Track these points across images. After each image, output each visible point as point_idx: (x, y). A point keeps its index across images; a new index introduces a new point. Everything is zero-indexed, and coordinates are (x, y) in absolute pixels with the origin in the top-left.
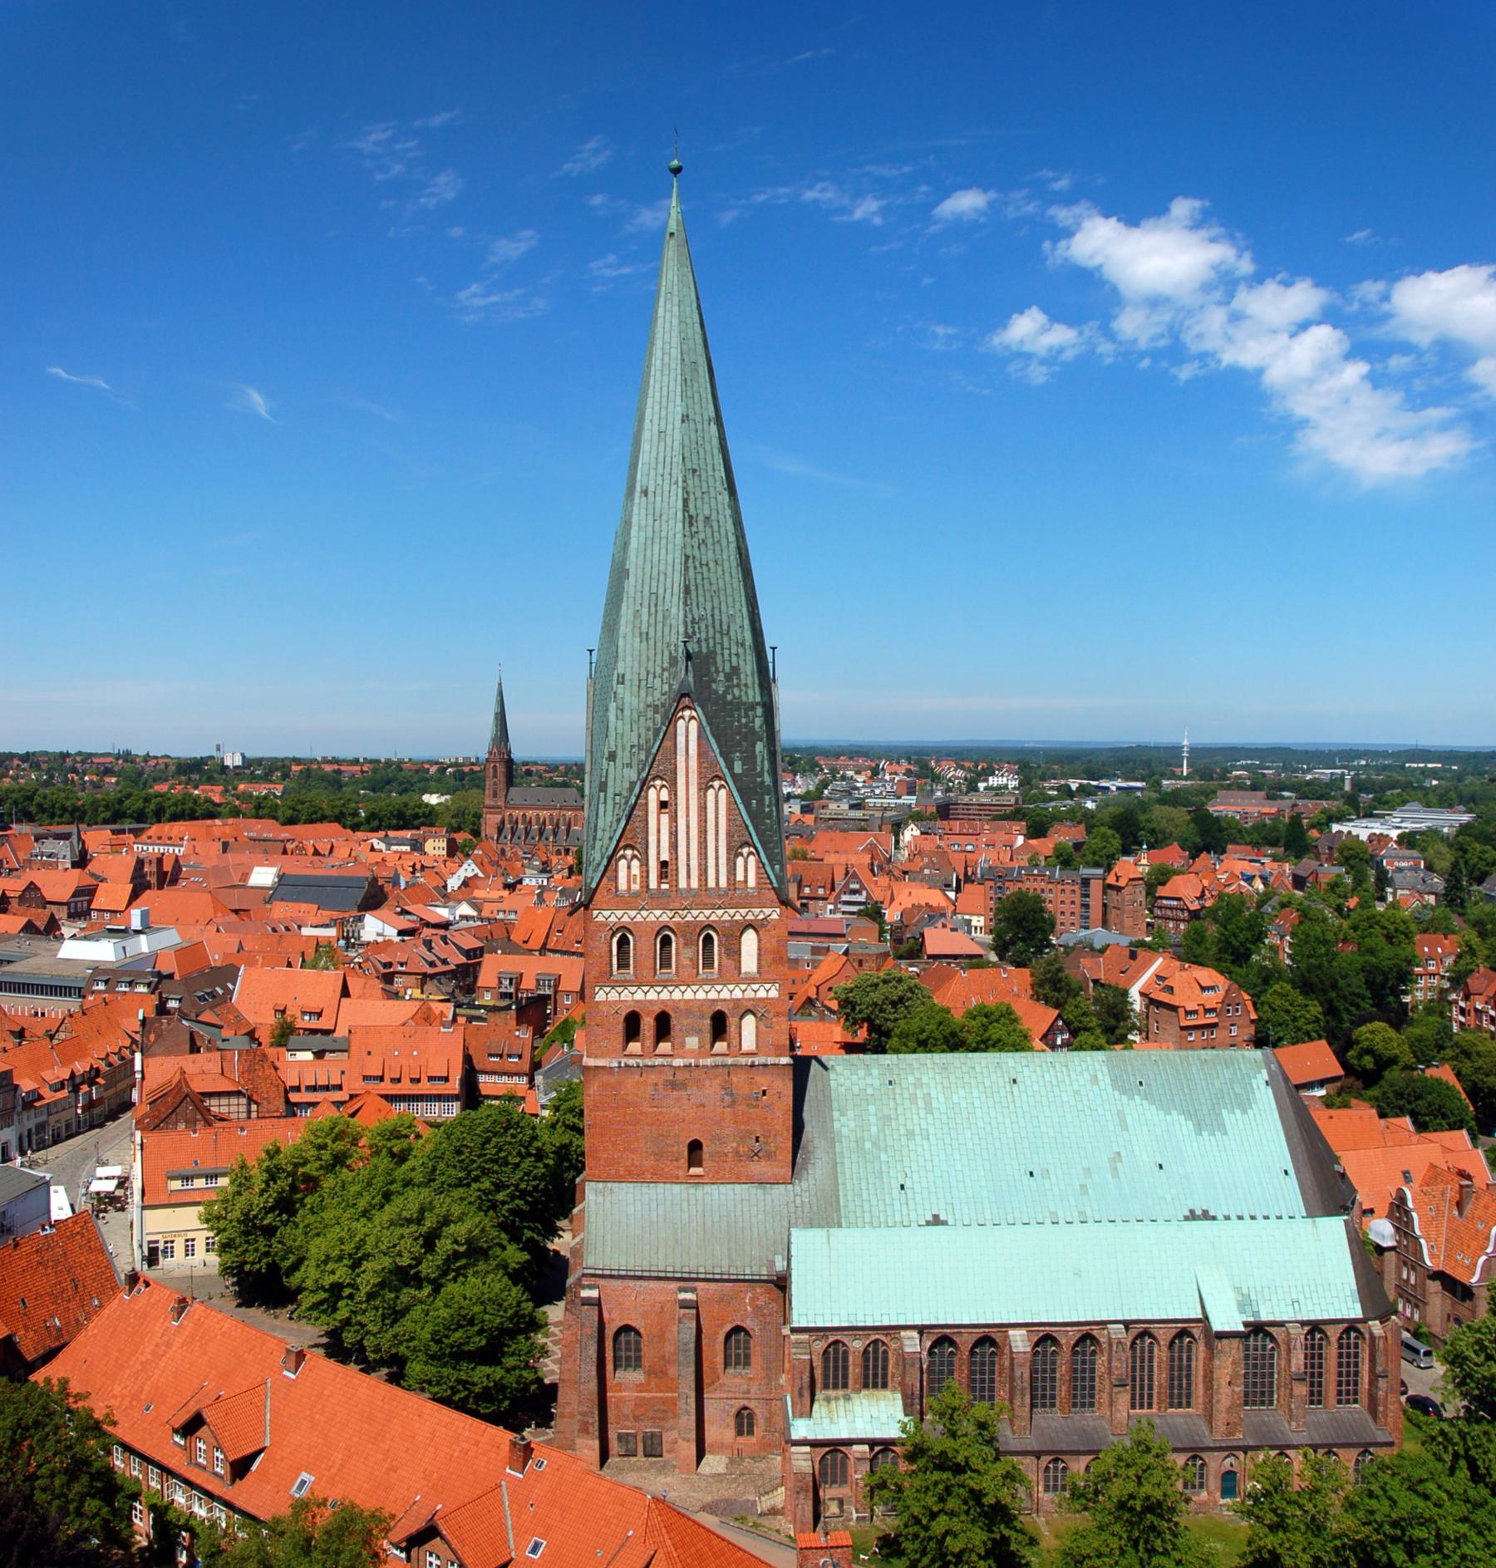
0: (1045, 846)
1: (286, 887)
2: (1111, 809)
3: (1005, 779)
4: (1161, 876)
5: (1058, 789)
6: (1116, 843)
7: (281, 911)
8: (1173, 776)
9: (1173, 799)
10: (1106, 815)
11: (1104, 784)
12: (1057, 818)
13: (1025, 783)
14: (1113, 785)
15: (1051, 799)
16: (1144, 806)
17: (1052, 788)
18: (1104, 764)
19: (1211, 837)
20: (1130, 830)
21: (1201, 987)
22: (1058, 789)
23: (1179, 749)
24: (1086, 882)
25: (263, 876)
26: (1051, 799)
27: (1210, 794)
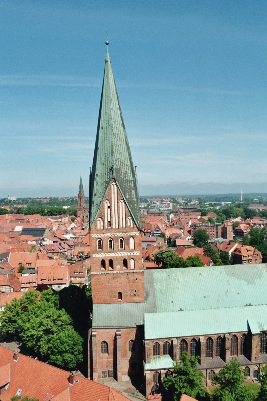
0: (206, 218)
1: (26, 231)
2: (223, 209)
3: (196, 202)
4: (235, 225)
5: (209, 204)
6: (224, 217)
7: (23, 237)
8: (238, 200)
9: (239, 206)
10: (221, 210)
11: (220, 203)
12: (209, 211)
13: (200, 203)
14: (223, 203)
15: (207, 207)
16: (231, 208)
17: (207, 204)
18: (220, 198)
19: (248, 214)
20: (228, 214)
21: (247, 251)
22: (209, 204)
23: (240, 194)
24: (217, 226)
25: (19, 229)
26: (207, 207)
27: (248, 205)
